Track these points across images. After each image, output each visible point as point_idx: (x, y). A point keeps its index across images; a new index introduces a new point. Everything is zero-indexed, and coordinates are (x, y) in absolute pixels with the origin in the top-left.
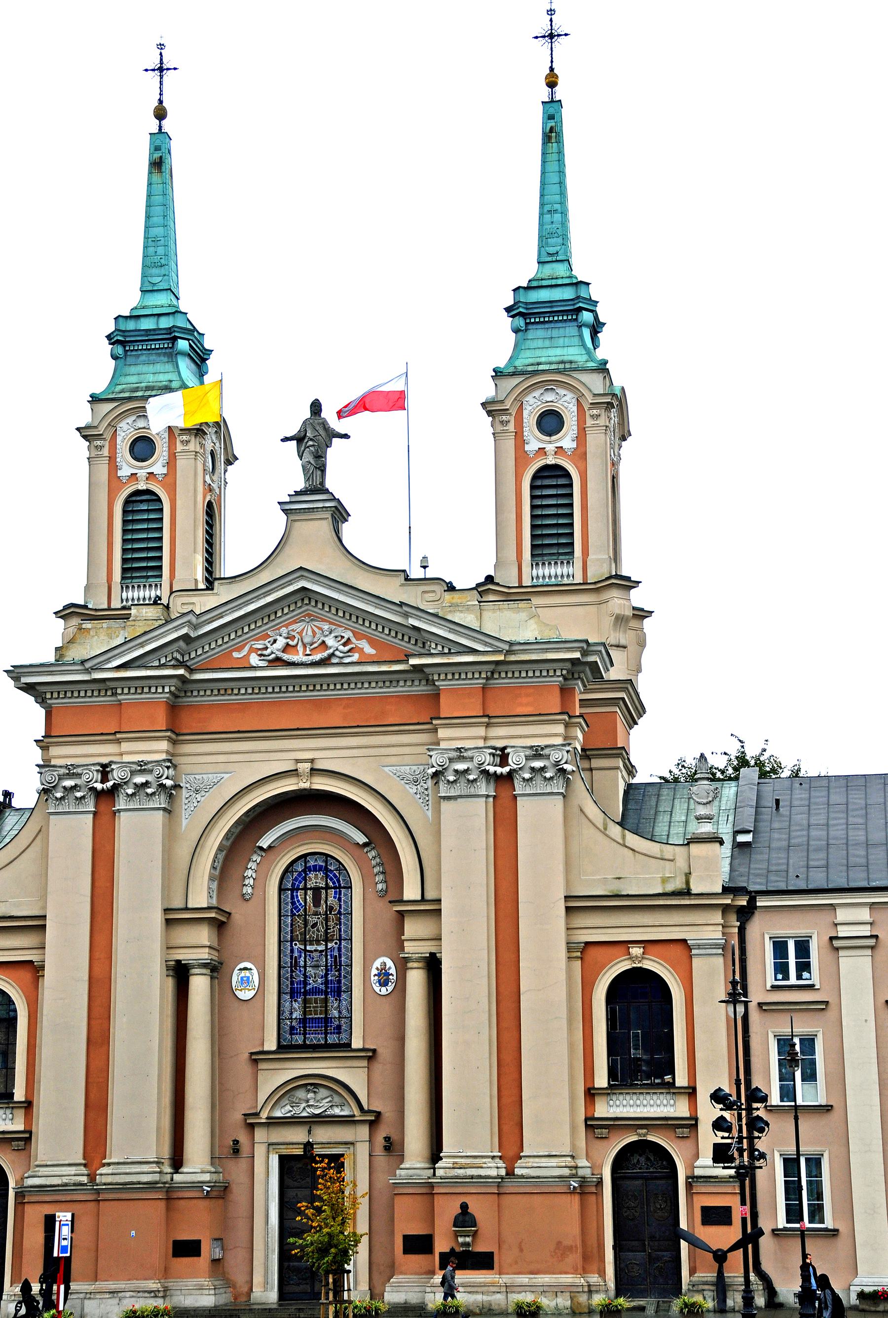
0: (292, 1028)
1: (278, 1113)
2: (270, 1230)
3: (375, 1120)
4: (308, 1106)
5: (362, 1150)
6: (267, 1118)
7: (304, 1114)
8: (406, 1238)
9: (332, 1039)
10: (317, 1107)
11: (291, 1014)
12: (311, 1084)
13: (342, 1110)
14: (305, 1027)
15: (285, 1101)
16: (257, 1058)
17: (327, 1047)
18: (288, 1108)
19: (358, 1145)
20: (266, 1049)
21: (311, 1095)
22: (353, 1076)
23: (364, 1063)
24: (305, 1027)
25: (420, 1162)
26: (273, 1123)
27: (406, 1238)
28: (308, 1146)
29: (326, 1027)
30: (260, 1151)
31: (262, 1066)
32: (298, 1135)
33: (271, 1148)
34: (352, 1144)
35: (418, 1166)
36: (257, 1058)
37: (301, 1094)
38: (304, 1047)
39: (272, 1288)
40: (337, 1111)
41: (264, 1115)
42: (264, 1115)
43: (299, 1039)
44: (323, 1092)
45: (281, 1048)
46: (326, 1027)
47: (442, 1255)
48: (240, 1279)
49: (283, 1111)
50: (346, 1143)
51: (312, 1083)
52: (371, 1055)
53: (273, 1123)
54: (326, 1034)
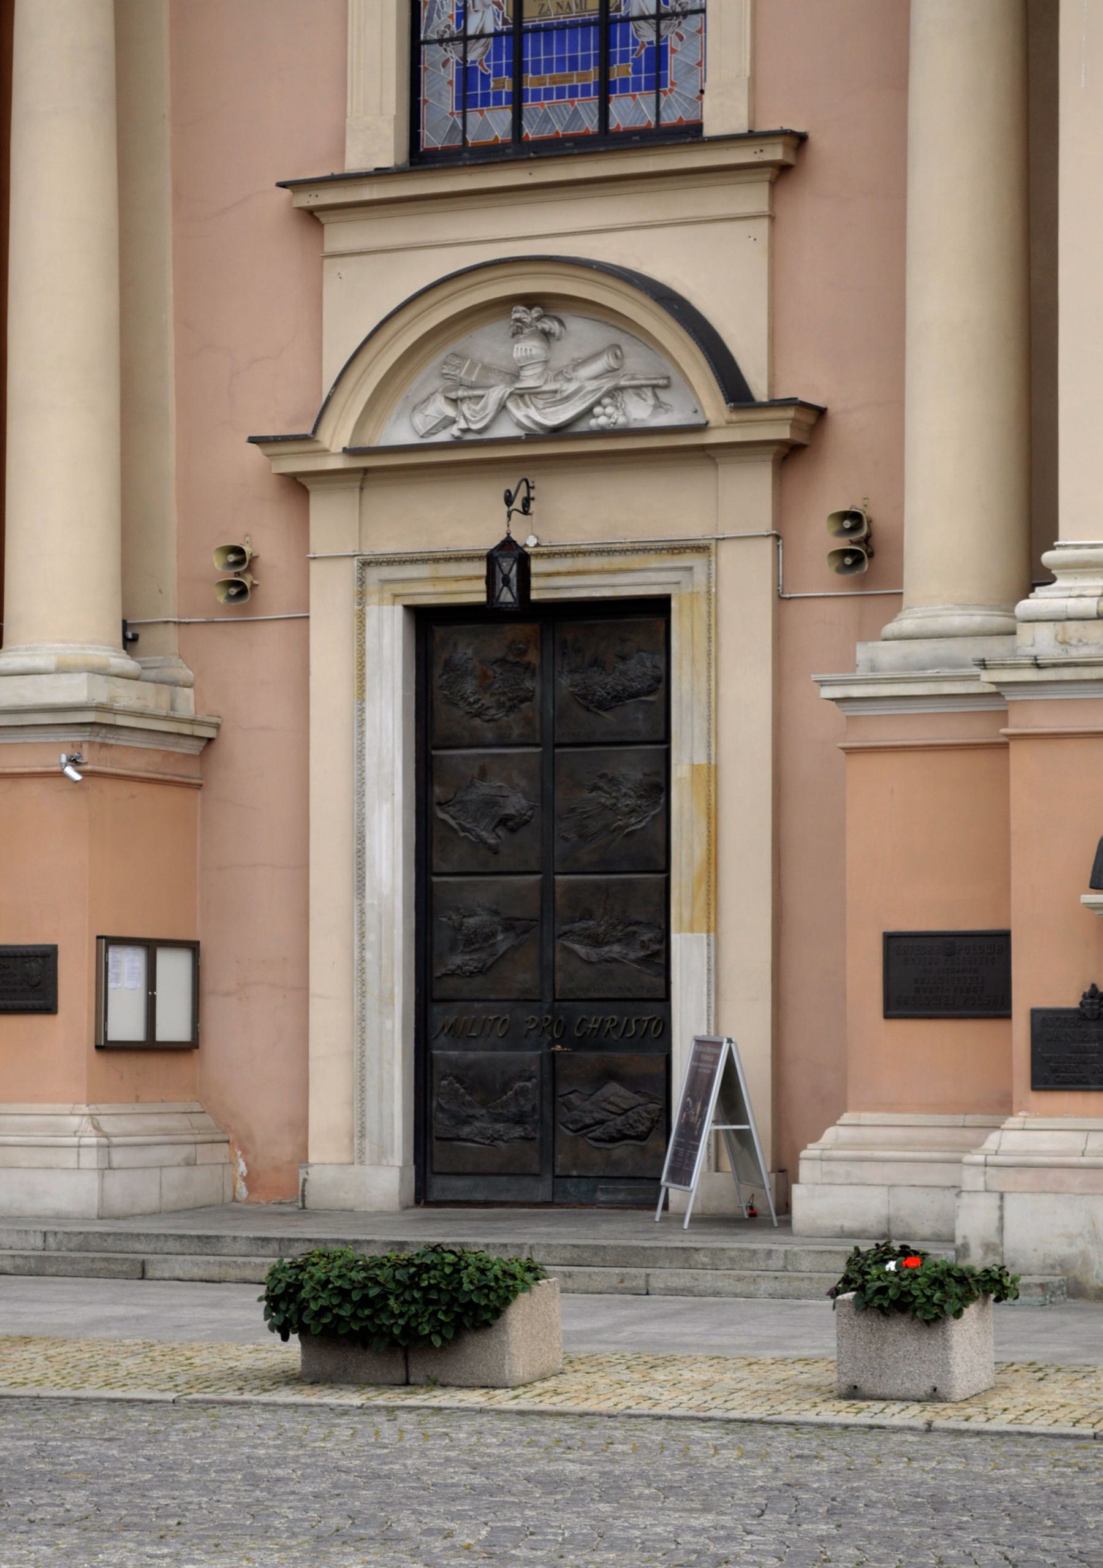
0: (466, 75)
1: (400, 431)
2: (371, 919)
3: (800, 442)
4: (521, 395)
5: (744, 583)
6: (350, 452)
7: (505, 430)
8: (899, 948)
9: (629, 111)
10: (558, 398)
11: (463, 15)
12: (529, 300)
13: (659, 405)
14: (517, 71)
15: (427, 378)
16: (321, 205)
17: (607, 140)
18: (440, 408)
19: (727, 554)
20: (354, 163)
21: (529, 347)
22: (706, 254)
23: (753, 197)
24: (517, 71)
25: (964, 605)
26: (375, 471)
27: (899, 948)
28: (509, 559)
29: (605, 62)
30: (330, 593)
31: (341, 236)
32: (471, 520)
33: (374, 574)
34: (701, 549)
35: (957, 620)
36: (321, 205)
37: (489, 344)
38: (519, 149)
39: (383, 1152)
40: (639, 412)
41: (338, 435)
42: (338, 435)
43: (493, 124)
44: (581, 334)
45: (419, 158)
46: (605, 62)
47: (1045, 1022)
48: (261, 1110)
49: (418, 420)
50: (676, 549)
51: (538, 303)
52: (784, 161)
53: (375, 471)
54: (605, 89)
